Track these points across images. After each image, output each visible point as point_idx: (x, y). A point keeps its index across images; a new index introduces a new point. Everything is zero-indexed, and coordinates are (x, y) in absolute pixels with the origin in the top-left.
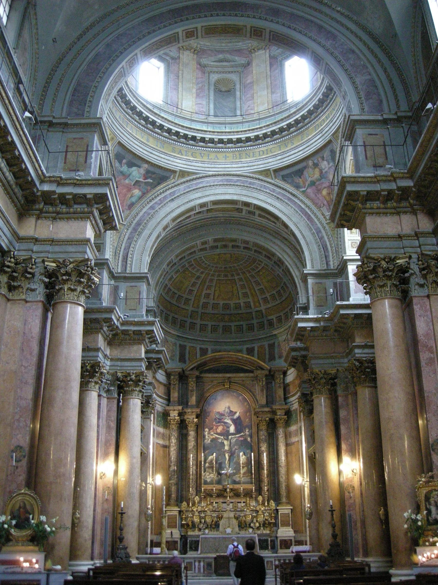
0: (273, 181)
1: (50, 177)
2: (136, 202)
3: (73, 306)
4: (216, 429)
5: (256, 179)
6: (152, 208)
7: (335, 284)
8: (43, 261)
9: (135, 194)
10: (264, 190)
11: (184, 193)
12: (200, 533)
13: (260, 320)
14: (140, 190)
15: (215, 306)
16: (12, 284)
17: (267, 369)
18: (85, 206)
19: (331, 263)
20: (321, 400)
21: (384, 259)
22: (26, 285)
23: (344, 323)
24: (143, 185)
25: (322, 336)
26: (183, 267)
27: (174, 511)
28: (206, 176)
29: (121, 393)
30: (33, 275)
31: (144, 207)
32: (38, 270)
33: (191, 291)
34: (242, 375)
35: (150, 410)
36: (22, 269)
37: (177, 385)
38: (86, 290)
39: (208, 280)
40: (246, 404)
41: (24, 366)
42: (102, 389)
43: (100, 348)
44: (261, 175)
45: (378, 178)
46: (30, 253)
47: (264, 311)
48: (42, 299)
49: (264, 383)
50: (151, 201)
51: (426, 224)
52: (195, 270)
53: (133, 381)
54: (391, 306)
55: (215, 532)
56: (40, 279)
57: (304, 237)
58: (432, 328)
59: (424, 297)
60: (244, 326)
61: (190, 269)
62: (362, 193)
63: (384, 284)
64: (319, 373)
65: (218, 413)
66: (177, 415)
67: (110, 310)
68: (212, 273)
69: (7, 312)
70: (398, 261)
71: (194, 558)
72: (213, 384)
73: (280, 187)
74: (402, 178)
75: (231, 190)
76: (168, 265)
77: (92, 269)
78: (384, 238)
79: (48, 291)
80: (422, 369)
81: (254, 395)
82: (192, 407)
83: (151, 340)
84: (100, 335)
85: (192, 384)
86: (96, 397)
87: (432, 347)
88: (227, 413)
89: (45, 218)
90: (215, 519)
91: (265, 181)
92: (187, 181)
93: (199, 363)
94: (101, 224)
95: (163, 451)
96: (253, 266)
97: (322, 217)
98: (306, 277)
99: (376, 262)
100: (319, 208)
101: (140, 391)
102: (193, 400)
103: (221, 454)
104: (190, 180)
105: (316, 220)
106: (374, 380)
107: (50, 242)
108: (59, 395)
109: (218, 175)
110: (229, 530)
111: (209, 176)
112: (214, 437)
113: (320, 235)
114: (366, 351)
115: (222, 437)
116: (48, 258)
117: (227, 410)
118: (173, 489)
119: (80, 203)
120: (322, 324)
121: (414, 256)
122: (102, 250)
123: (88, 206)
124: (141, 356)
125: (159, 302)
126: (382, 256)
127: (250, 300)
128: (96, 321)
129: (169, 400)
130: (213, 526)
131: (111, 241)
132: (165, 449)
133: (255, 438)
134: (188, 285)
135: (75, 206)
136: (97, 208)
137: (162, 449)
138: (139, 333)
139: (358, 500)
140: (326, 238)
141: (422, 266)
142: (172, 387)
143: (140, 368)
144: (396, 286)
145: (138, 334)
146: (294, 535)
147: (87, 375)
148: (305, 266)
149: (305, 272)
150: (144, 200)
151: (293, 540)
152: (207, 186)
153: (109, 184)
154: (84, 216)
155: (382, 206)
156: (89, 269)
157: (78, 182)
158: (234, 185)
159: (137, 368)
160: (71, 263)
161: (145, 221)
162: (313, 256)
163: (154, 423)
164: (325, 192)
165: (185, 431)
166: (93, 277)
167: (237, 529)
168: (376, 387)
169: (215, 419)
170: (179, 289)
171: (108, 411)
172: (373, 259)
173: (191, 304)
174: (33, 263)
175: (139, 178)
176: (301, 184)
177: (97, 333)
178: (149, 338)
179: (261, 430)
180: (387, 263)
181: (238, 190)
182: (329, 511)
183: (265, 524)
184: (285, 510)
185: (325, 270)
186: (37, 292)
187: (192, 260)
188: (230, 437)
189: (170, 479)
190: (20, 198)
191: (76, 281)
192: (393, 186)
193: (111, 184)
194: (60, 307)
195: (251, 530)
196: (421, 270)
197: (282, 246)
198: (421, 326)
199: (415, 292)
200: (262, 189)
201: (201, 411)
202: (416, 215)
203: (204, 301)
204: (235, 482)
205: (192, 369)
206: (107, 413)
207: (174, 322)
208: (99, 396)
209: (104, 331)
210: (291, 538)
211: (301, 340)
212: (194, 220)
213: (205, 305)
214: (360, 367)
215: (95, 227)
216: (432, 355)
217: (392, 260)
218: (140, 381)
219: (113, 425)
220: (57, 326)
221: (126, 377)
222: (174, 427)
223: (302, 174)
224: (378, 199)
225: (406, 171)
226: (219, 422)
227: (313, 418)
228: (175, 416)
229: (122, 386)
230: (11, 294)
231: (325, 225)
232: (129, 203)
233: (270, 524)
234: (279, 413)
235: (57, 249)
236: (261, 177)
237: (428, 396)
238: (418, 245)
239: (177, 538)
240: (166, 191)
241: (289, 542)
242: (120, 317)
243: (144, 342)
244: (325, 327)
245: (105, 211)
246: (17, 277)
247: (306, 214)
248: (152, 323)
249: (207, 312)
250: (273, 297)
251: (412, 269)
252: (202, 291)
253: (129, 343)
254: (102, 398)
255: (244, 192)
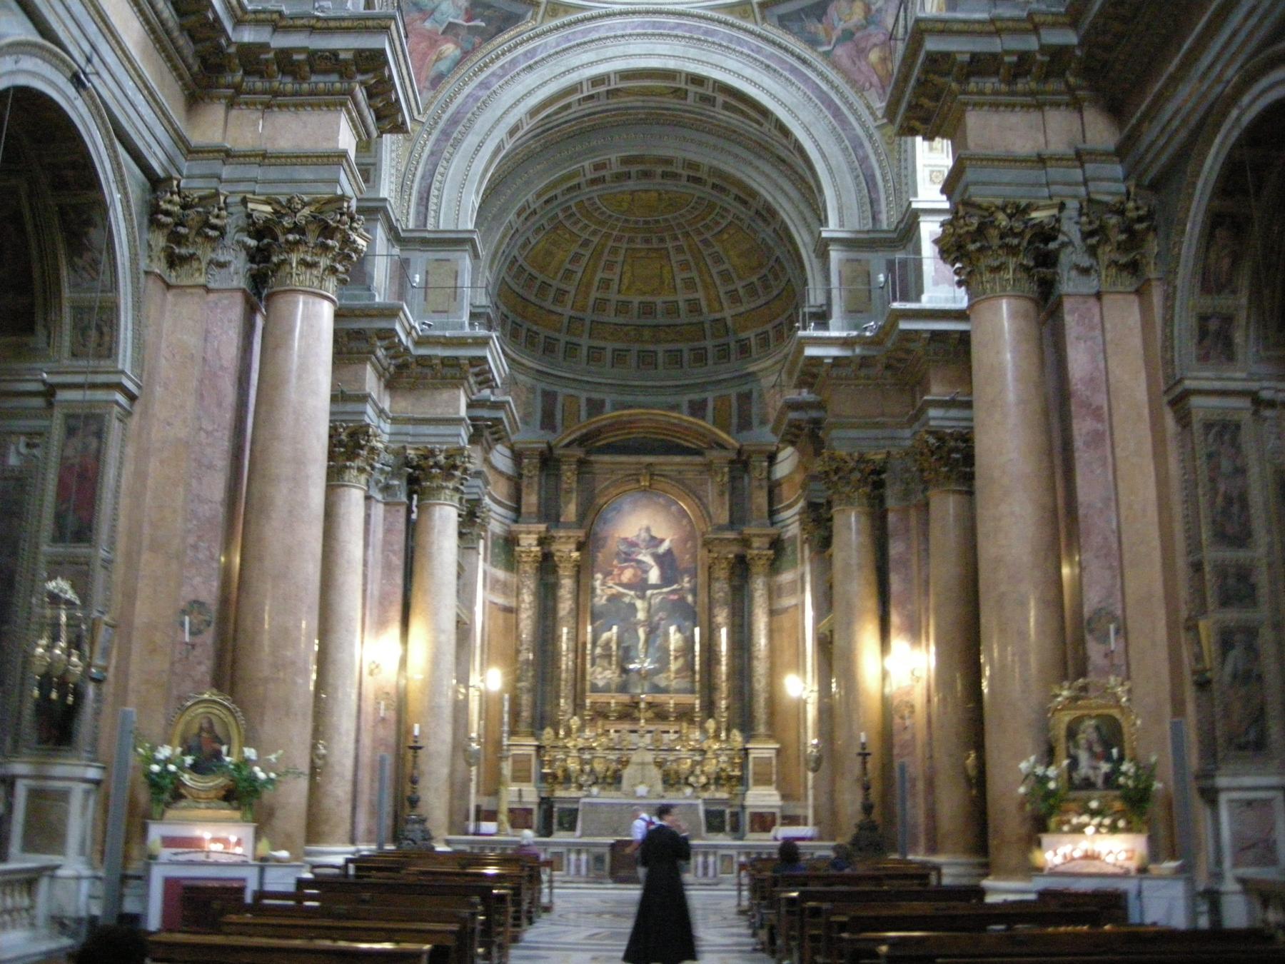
0: (757, 29)
1: (255, 12)
2: (449, 71)
3: (311, 299)
4: (620, 575)
5: (720, 22)
6: (484, 85)
7: (890, 266)
8: (244, 202)
9: (447, 53)
10: (738, 48)
11: (557, 53)
12: (580, 794)
13: (722, 341)
14: (456, 44)
15: (623, 307)
16: (177, 251)
17: (734, 448)
18: (334, 77)
19: (883, 217)
20: (849, 517)
21: (1003, 209)
22: (206, 253)
23: (908, 351)
24: (463, 33)
25: (857, 378)
26: (552, 219)
27: (525, 746)
28: (608, 15)
29: (415, 492)
30: (222, 231)
31: (466, 84)
32: (232, 221)
33: (568, 274)
34: (678, 459)
35: (476, 530)
36: (197, 219)
37: (536, 479)
38: (338, 266)
39: (606, 251)
40: (685, 522)
41: (207, 433)
42: (372, 483)
43: (369, 395)
44: (731, 13)
45: (998, 24)
46: (214, 183)
47: (729, 322)
48: (243, 285)
49: (726, 479)
50: (481, 70)
51: (1101, 132)
52: (581, 225)
53: (441, 468)
54: (1013, 315)
55: (613, 793)
56: (238, 242)
57: (823, 156)
58: (1102, 365)
59: (1089, 295)
60: (686, 355)
61: (567, 224)
62: (959, 58)
63: (1002, 264)
64: (848, 458)
65: (625, 540)
66: (535, 543)
67: (391, 312)
68: (615, 233)
69: (167, 314)
70: (1034, 215)
71: (568, 844)
72: (614, 478)
73: (774, 43)
74: (1054, 25)
75: (662, 47)
76: (519, 215)
77: (352, 219)
78: (1005, 160)
79: (255, 266)
80: (1076, 455)
81: (703, 504)
82: (568, 526)
83: (481, 378)
84: (369, 367)
85: (568, 475)
86: (361, 502)
87: (1099, 408)
88: (644, 540)
89: (246, 104)
90: (614, 766)
91: (739, 28)
92: (564, 26)
93: (584, 431)
94: (370, 118)
95: (505, 620)
96: (707, 221)
97: (867, 112)
98: (827, 245)
99: (986, 214)
100: (860, 90)
101: (456, 490)
102: (570, 511)
103: (629, 628)
104: (570, 24)
105: (852, 119)
106: (969, 478)
107: (258, 160)
108: (280, 495)
109: (634, 13)
110: (642, 790)
111: (614, 14)
112: (614, 591)
113: (861, 153)
114: (953, 413)
115: (632, 593)
116: (254, 193)
117: (644, 535)
118: (526, 699)
119: (326, 72)
120: (858, 350)
121: (1072, 205)
122: (372, 177)
123: (341, 77)
124: (458, 412)
125: (499, 295)
126: (999, 202)
127: (700, 295)
128: (359, 335)
129: (517, 510)
130: (609, 780)
131: (392, 159)
132: (509, 615)
133: (703, 597)
134: (562, 262)
135: (314, 78)
136: (362, 83)
137: (501, 615)
138: (452, 363)
139: (921, 735)
140: (873, 159)
141: (1087, 228)
142: (525, 482)
143: (455, 439)
144: (1027, 269)
145: (452, 366)
146: (780, 803)
147: (341, 453)
148: (823, 221)
149: (824, 235)
150: (466, 68)
151: (778, 815)
152: (607, 38)
153: (388, 28)
154: (335, 101)
155: (1004, 87)
156: (345, 218)
157: (319, 24)
158: (668, 35)
159: (450, 439)
160: (305, 205)
161: (469, 115)
162: (844, 199)
163: (485, 560)
164: (874, 56)
165: (551, 579)
166: (354, 236)
167: (659, 787)
168: (971, 493)
169: (618, 554)
170: (542, 269)
171: (388, 531)
172: (979, 207)
173: (570, 303)
174: (222, 205)
175: (456, 17)
176: (822, 35)
177: (363, 361)
178: (477, 375)
179: (718, 579)
180: (1010, 217)
181: (678, 48)
182: (860, 754)
183: (719, 779)
184: (763, 750)
185: (868, 232)
186: (232, 269)
187: (572, 203)
188: (649, 592)
189: (518, 679)
190: (191, 60)
191: (316, 245)
192: (1031, 44)
193: (393, 27)
194: (281, 303)
195: (688, 791)
196: (1086, 235)
197: (775, 175)
198: (1079, 361)
199: (1069, 283)
200: (733, 46)
201: (588, 536)
202: (1080, 111)
203: (599, 296)
204: (656, 689)
205: (568, 445)
206: (384, 537)
207: (531, 338)
208: (368, 498)
209: (377, 358)
211: (811, 386)
212: (577, 115)
213: (600, 305)
214: (938, 447)
215: (358, 125)
216: (1099, 426)
217: (1020, 211)
218: (455, 467)
219: (398, 561)
220: (275, 344)
221: (426, 458)
222: (529, 568)
223: (825, 13)
224: (996, 73)
225: (1062, 10)
226: (626, 561)
227: (831, 556)
228: (530, 545)
229: (417, 478)
230: (174, 274)
231: (872, 130)
232: (432, 73)
233: (730, 778)
234: (756, 543)
235: (273, 173)
236: (730, 19)
237: (1086, 516)
238: (1081, 179)
239: (531, 803)
240: (516, 46)
242: (413, 327)
243: (466, 385)
244: (863, 358)
245: (381, 91)
246: (186, 237)
247: (830, 104)
248: (484, 342)
249: (606, 319)
250: (752, 290)
251: (1064, 234)
252: (594, 272)
253: (433, 384)
254: (373, 502)
255: (692, 52)
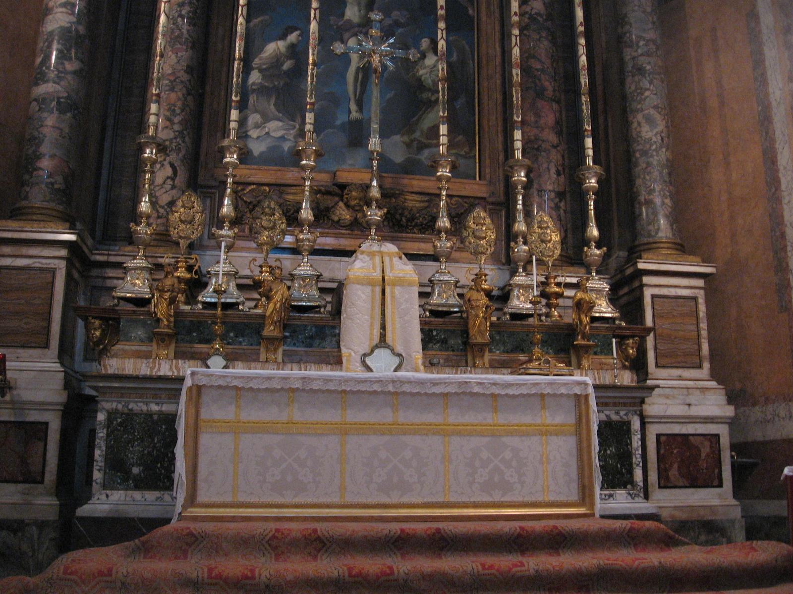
146: (730, 411)
151: (725, 441)
210: (712, 429)
239: (42, 406)
241: (705, 450)
